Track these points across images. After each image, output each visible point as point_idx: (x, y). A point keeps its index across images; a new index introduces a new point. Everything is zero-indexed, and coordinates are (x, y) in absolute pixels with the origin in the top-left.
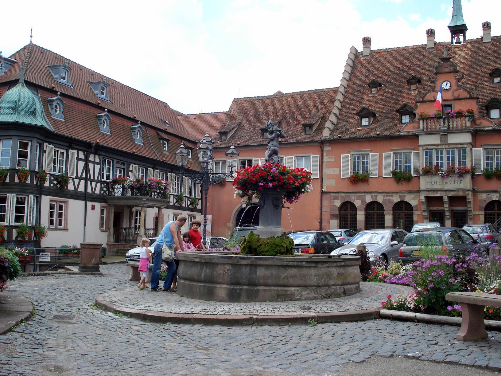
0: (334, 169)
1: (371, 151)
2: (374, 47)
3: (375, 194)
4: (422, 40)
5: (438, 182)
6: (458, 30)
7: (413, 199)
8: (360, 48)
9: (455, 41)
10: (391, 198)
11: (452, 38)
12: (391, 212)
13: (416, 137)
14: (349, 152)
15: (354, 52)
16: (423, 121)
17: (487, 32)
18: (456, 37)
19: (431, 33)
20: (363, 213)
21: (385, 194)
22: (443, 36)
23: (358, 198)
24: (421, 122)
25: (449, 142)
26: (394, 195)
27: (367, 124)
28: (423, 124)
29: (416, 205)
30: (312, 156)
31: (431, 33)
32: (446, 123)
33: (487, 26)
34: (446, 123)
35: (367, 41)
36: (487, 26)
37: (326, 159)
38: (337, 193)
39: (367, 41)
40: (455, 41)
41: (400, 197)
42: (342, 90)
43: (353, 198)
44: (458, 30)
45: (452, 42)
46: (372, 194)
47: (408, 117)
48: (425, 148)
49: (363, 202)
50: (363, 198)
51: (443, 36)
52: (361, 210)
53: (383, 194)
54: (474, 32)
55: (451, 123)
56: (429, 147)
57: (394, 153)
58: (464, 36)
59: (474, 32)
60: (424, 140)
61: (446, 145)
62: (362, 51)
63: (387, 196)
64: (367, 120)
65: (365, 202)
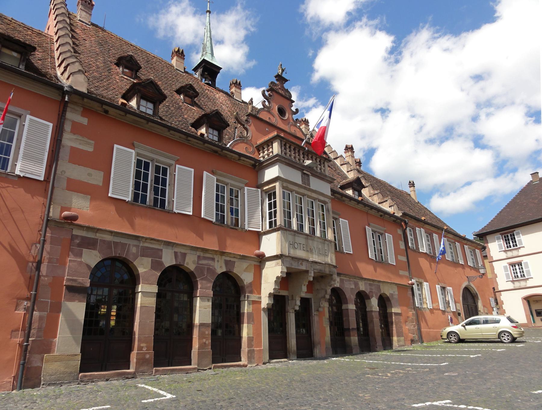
0: (91, 171)
1: (178, 162)
5: (301, 245)
7: (246, 270)
10: (210, 262)
14: (132, 146)
21: (202, 254)
23: (145, 252)
25: (312, 187)
26: (216, 257)
29: (251, 284)
30: (29, 117)
37: (69, 140)
41: (227, 263)
43: (134, 250)
53: (198, 253)
63: (205, 258)
65: (161, 264)
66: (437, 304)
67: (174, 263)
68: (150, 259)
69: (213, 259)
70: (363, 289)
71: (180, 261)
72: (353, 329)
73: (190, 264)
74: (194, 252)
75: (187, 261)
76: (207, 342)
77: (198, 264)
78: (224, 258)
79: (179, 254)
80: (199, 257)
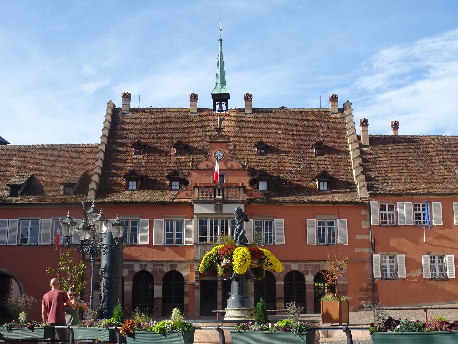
1: (142, 217)
2: (134, 104)
3: (145, 263)
4: (186, 104)
6: (221, 99)
7: (185, 268)
8: (119, 104)
9: (217, 108)
10: (161, 267)
11: (215, 105)
12: (162, 282)
13: (191, 206)
15: (112, 107)
16: (199, 190)
17: (248, 103)
18: (218, 105)
19: (194, 98)
20: (131, 283)
21: (156, 263)
22: (206, 102)
24: (196, 190)
25: (224, 212)
27: (135, 187)
28: (199, 192)
31: (194, 98)
32: (221, 194)
33: (248, 98)
34: (221, 194)
35: (127, 97)
36: (248, 98)
38: (310, 261)
39: (127, 97)
40: (217, 108)
41: (171, 266)
42: (103, 148)
44: (221, 99)
45: (214, 110)
46: (141, 263)
47: (178, 183)
48: (200, 216)
49: (131, 271)
50: (132, 266)
51: (206, 102)
52: (128, 280)
53: (154, 263)
54: (236, 102)
55: (225, 193)
56: (203, 216)
57: (165, 220)
58: (227, 105)
59: (236, 102)
60: (199, 209)
61: (221, 214)
62: (121, 106)
63: (158, 265)
64: (135, 183)
65: (134, 271)
66: (420, 273)
67: (140, 270)
68: (128, 270)
69: (163, 265)
70: (296, 269)
71: (143, 269)
72: (279, 298)
73: (149, 269)
74: (150, 263)
75: (147, 268)
76: (159, 306)
77: (153, 268)
78: (169, 263)
79: (143, 265)
80: (154, 265)
